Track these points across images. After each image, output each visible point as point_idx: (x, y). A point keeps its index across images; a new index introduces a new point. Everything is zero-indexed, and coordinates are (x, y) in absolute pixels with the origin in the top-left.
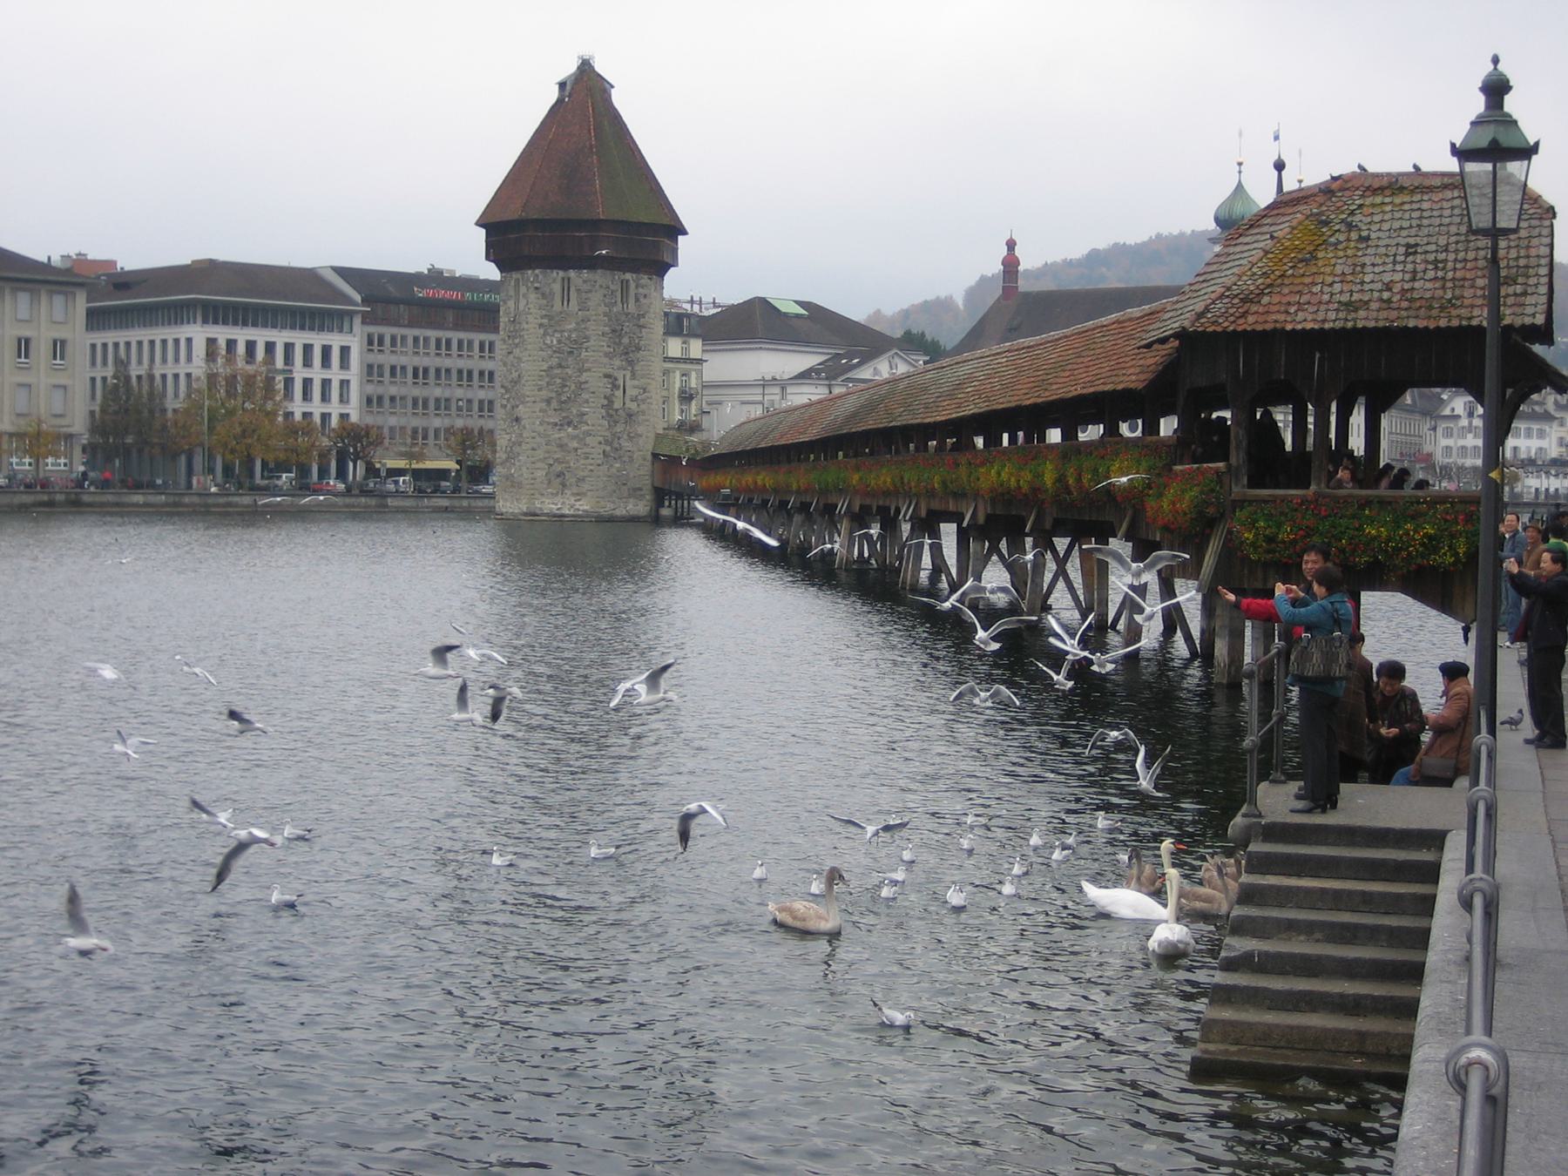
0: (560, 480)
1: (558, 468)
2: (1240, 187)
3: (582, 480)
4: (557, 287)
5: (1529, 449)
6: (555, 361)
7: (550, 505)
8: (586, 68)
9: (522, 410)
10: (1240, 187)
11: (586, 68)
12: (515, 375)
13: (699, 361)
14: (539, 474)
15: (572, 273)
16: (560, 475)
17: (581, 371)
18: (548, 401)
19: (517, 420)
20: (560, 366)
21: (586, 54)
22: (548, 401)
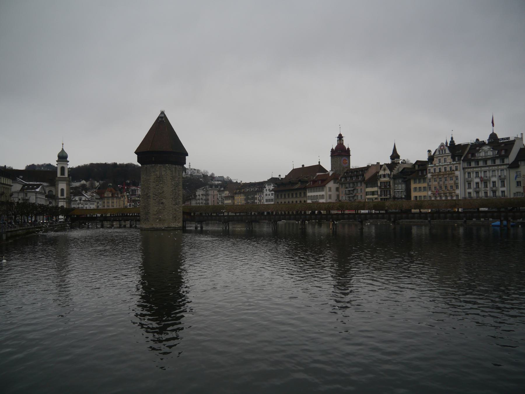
0: (175, 218)
1: (175, 216)
2: (63, 149)
3: (179, 218)
4: (174, 169)
5: (86, 207)
6: (173, 188)
7: (173, 225)
8: (162, 113)
9: (164, 201)
10: (63, 149)
11: (162, 113)
12: (160, 191)
13: (11, 186)
14: (171, 217)
15: (177, 166)
16: (175, 217)
17: (179, 191)
18: (172, 198)
19: (162, 203)
20: (175, 190)
21: (163, 109)
22: (172, 198)
